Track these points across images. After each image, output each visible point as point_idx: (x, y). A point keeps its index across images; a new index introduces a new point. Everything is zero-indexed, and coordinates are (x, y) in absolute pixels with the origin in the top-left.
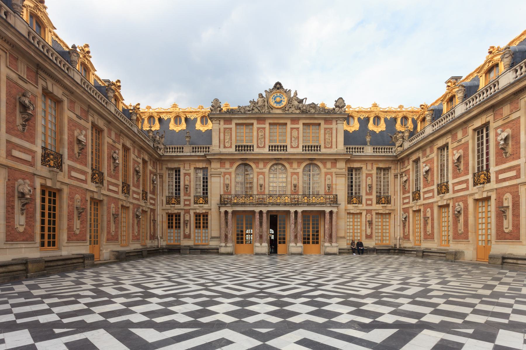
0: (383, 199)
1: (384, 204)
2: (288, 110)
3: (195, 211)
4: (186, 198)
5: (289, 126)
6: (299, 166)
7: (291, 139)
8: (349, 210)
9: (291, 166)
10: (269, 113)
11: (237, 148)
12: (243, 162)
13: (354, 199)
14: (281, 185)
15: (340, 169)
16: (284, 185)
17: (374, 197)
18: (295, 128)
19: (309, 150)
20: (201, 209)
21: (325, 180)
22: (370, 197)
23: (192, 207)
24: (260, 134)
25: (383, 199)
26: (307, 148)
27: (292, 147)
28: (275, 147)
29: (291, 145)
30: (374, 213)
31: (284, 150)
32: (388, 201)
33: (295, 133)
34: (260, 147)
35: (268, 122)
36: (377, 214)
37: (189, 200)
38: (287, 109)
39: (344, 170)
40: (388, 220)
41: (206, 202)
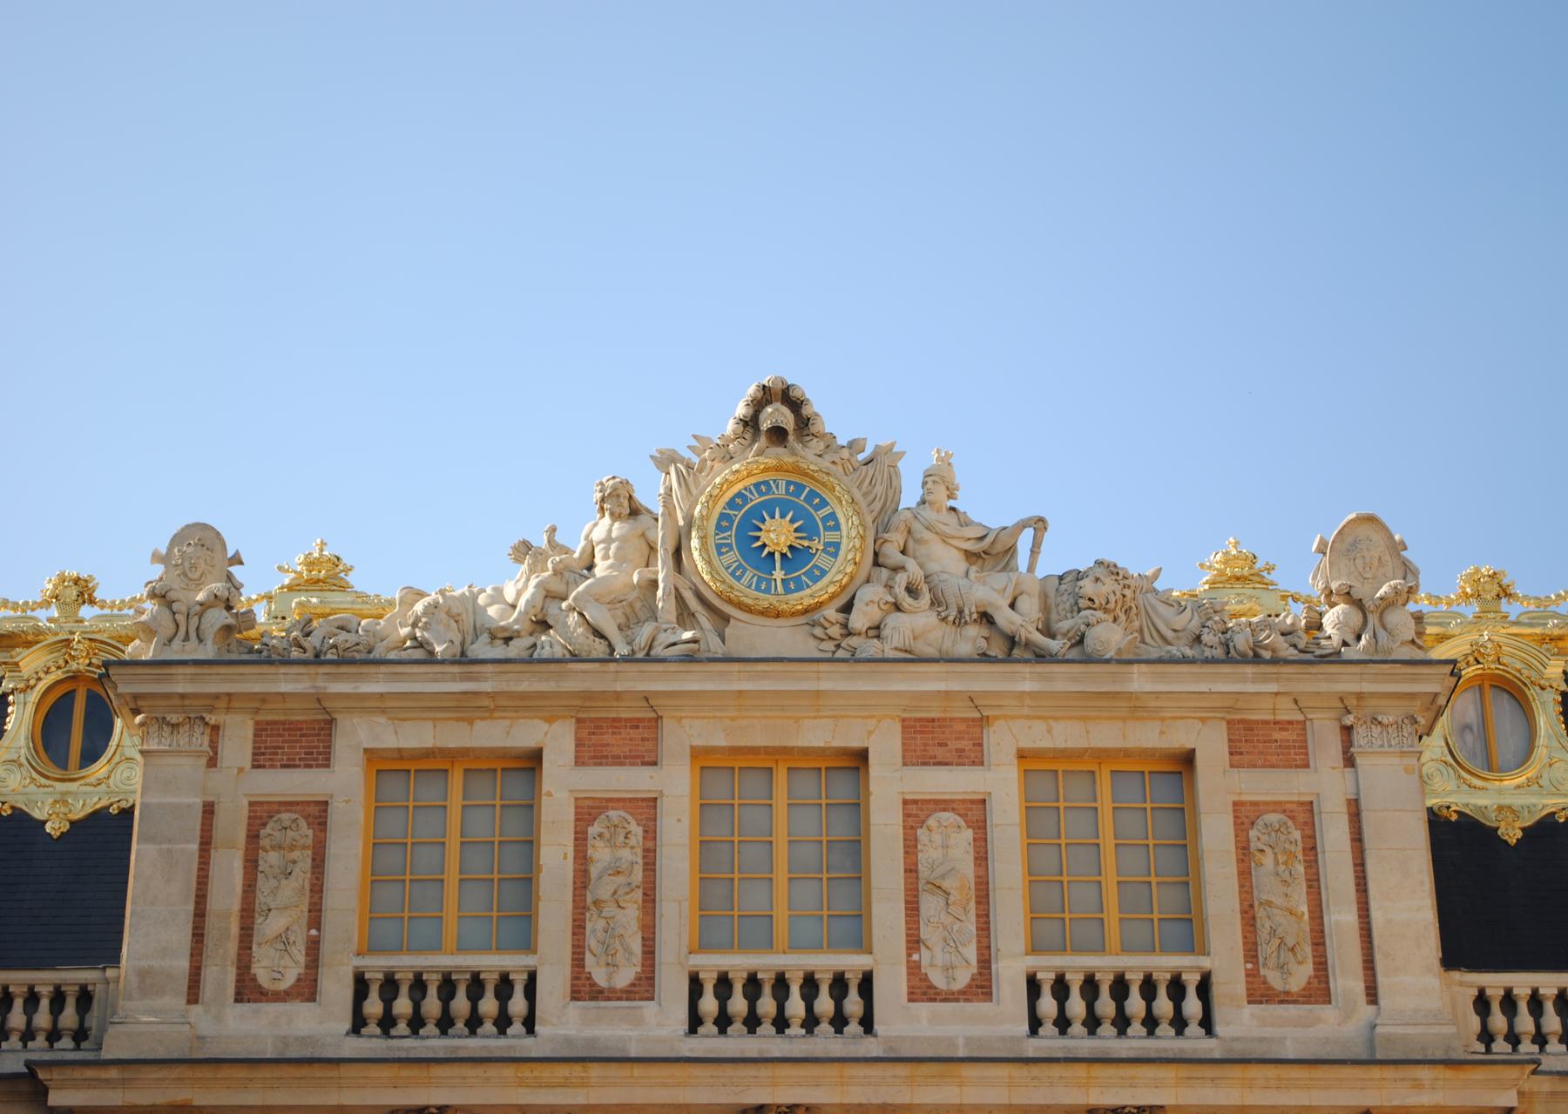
2: (876, 630)
7: (913, 908)
19: (1093, 1023)
24: (601, 854)
27: (922, 990)
28: (753, 985)
29: (914, 969)
33: (948, 846)
34: (597, 994)
35: (684, 734)
38: (858, 620)
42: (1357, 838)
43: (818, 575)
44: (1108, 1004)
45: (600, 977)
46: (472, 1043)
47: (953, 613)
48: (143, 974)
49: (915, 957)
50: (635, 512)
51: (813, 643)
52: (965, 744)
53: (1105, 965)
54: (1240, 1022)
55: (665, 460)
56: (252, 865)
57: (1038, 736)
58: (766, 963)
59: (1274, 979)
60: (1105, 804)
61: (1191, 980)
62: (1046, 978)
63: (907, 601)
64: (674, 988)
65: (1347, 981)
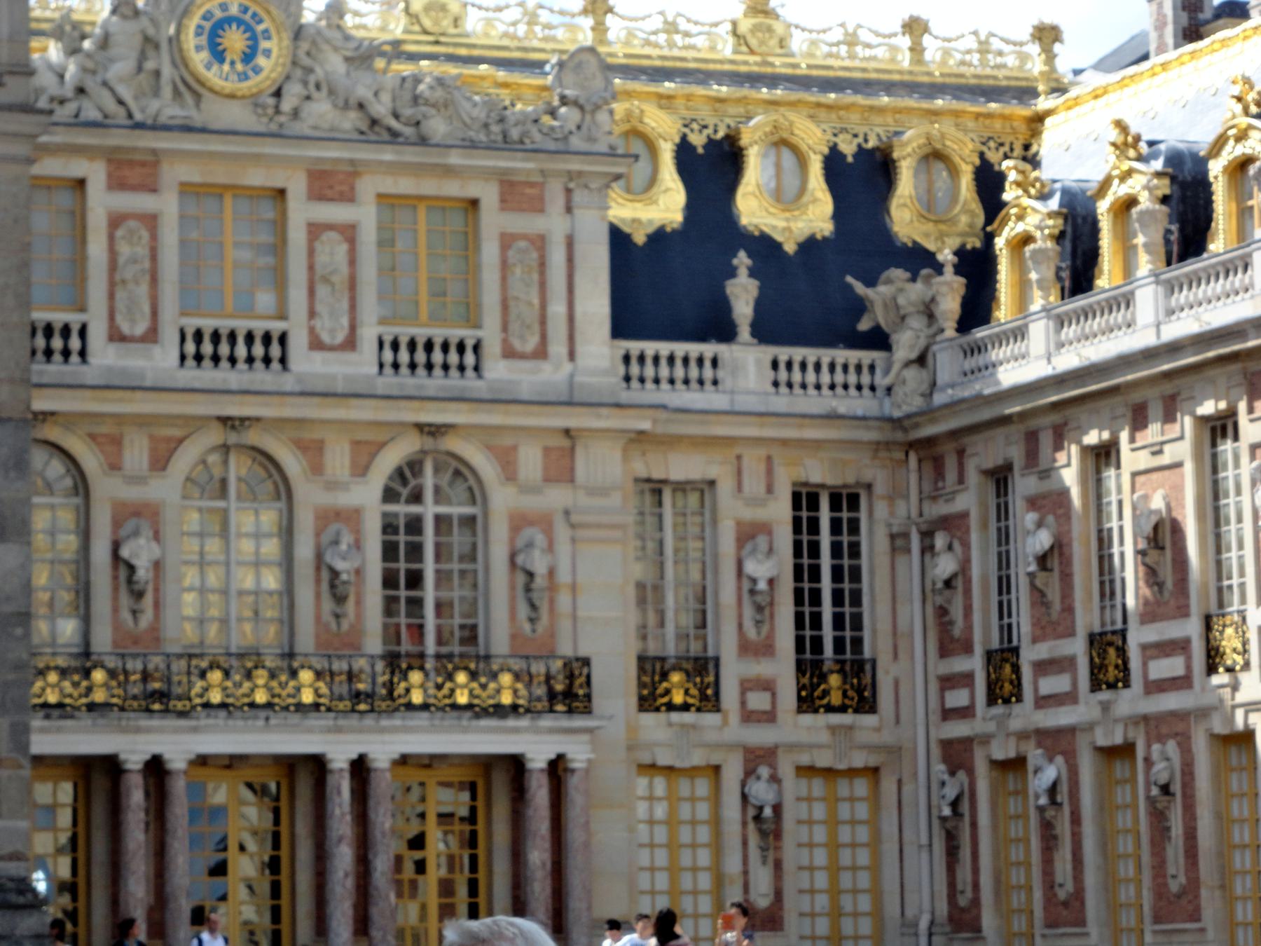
0: (834, 680)
1: (842, 709)
2: (296, 113)
6: (361, 470)
7: (312, 292)
9: (317, 468)
14: (249, 583)
15: (592, 491)
18: (330, 227)
22: (761, 668)
24: (124, 250)
25: (834, 680)
26: (404, 357)
27: (317, 344)
29: (312, 330)
30: (786, 769)
31: (267, 360)
32: (860, 690)
33: (333, 253)
35: (175, 173)
38: (287, 105)
39: (615, 500)
42: (570, 260)
44: (416, 355)
45: (125, 328)
46: (51, 368)
49: (313, 322)
51: (254, 118)
52: (345, 188)
53: (421, 333)
54: (497, 369)
57: (392, 185)
58: (225, 325)
59: (517, 345)
60: (422, 227)
61: (470, 344)
62: (388, 339)
63: (315, 94)
65: (558, 348)
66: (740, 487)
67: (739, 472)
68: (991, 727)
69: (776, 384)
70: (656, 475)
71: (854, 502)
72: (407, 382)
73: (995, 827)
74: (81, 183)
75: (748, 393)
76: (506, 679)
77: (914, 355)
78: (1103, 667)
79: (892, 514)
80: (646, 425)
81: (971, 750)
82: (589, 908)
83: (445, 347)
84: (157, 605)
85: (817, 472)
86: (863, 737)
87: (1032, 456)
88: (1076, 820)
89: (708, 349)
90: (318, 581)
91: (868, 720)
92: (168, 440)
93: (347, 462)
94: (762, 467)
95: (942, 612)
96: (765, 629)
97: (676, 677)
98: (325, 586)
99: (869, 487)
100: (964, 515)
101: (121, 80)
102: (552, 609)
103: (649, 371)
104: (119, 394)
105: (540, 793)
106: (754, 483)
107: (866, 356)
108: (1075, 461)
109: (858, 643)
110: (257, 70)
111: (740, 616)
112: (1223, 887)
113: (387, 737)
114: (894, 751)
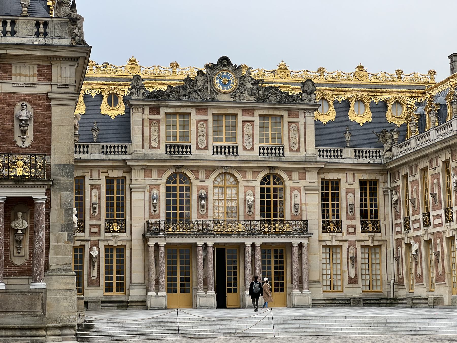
0: (370, 225)
1: (372, 232)
3: (106, 243)
4: (94, 222)
5: (241, 118)
6: (255, 178)
7: (243, 137)
8: (325, 241)
9: (245, 177)
10: (213, 100)
11: (168, 150)
12: (177, 171)
13: (331, 224)
15: (311, 182)
16: (234, 204)
17: (357, 222)
20: (115, 240)
21: (291, 197)
22: (352, 222)
23: (102, 237)
24: (200, 129)
25: (370, 225)
26: (265, 151)
27: (245, 149)
28: (221, 148)
29: (243, 146)
30: (358, 246)
31: (233, 153)
33: (248, 128)
34: (200, 149)
35: (211, 112)
36: (362, 246)
37: (98, 226)
38: (237, 95)
39: (316, 184)
40: (378, 256)
41: (123, 230)
42: (305, 128)
43: (231, 87)
47: (250, 94)
48: (136, 145)
50: (203, 75)
54: (287, 154)
55: (207, 66)
56: (150, 129)
57: (262, 112)
59: (293, 148)
63: (244, 92)
64: (210, 148)
65: (302, 149)
66: (347, 181)
67: (347, 177)
68: (405, 236)
69: (356, 156)
70: (327, 178)
71: (375, 184)
72: (266, 158)
73: (406, 259)
74: (190, 113)
75: (349, 158)
76: (288, 225)
77: (389, 149)
78: (425, 221)
79: (384, 186)
80: (323, 166)
81: (401, 241)
82: (308, 278)
83: (275, 150)
84: (207, 209)
85: (366, 177)
86: (376, 238)
87: (411, 172)
88: (421, 258)
89: (339, 149)
90: (245, 203)
91: (379, 234)
92: (210, 171)
93: (252, 176)
94: (352, 175)
95: (395, 208)
96: (353, 213)
97: (331, 224)
98: (246, 204)
99: (378, 180)
100: (399, 186)
101: (199, 90)
102: (301, 209)
103: (325, 154)
104: (197, 161)
105: (296, 252)
106: (350, 179)
107: (378, 149)
108: (419, 173)
109: (376, 217)
110: (231, 87)
111: (347, 210)
112: (450, 273)
113: (259, 239)
114: (385, 241)
